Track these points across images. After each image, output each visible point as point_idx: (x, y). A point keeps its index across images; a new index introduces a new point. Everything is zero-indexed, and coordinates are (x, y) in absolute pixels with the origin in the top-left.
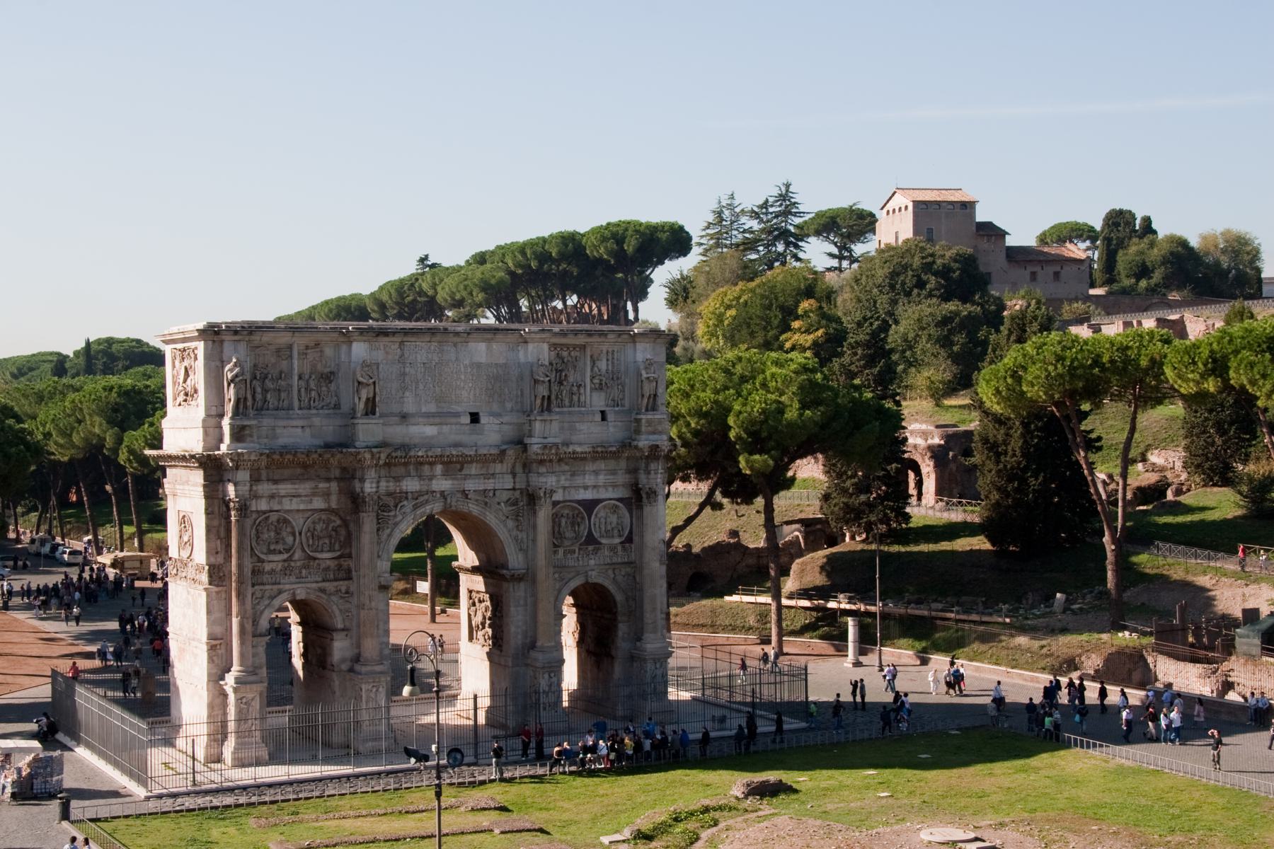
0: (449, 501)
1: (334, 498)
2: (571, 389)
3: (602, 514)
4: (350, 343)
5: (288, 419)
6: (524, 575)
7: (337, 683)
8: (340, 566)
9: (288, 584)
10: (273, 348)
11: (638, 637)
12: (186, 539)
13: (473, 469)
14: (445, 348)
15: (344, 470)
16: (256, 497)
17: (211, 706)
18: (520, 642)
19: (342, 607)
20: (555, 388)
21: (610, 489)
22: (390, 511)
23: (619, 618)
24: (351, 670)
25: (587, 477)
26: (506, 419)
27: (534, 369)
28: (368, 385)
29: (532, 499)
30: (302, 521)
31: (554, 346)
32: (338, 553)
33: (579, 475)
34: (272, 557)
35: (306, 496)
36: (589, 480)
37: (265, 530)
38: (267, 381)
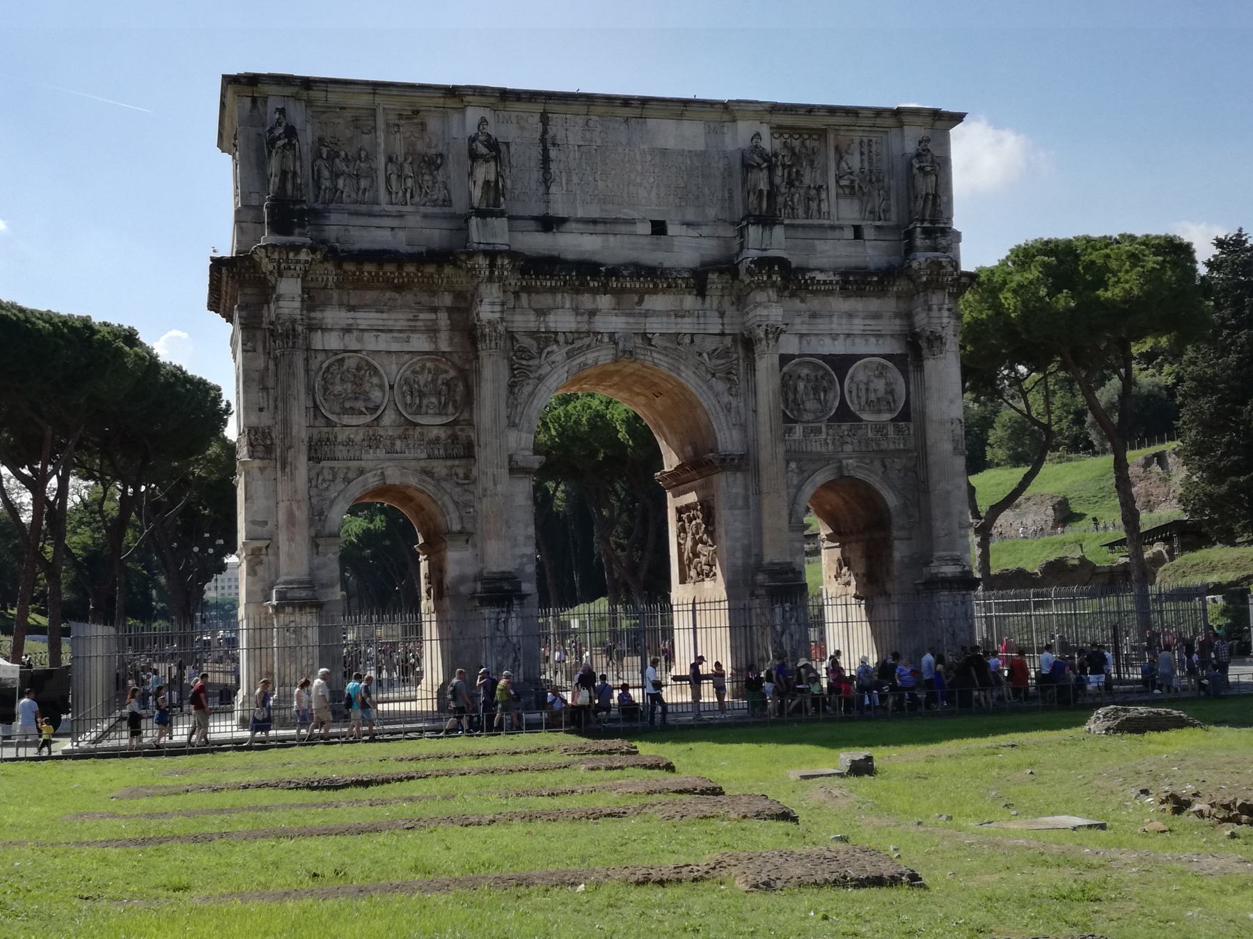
0: (621, 346)
2: (807, 193)
3: (861, 377)
4: (462, 110)
5: (370, 215)
6: (742, 457)
8: (454, 438)
9: (371, 458)
10: (348, 114)
11: (924, 559)
15: (459, 295)
18: (739, 562)
19: (456, 498)
21: (873, 340)
22: (531, 358)
23: (895, 533)
25: (835, 319)
26: (705, 230)
29: (748, 343)
30: (394, 368)
31: (778, 130)
32: (451, 419)
33: (822, 316)
34: (346, 420)
35: (400, 331)
36: (838, 325)
37: (338, 380)
38: (337, 161)
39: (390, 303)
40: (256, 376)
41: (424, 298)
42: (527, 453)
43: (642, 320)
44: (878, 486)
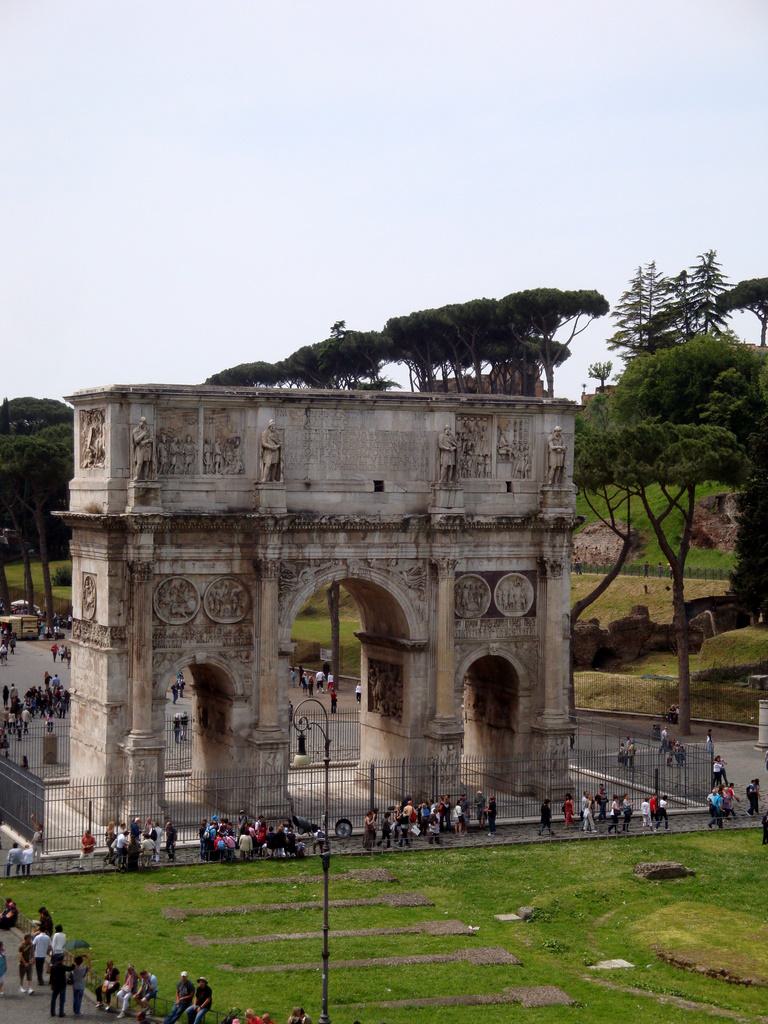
1: (236, 563)
6: (425, 644)
8: (240, 631)
9: (189, 645)
11: (539, 711)
12: (89, 600)
13: (377, 538)
14: (351, 415)
16: (160, 560)
17: (110, 769)
18: (419, 714)
20: (461, 456)
21: (515, 561)
23: (521, 693)
24: (250, 735)
25: (491, 548)
27: (441, 436)
28: (273, 451)
29: (434, 568)
31: (460, 416)
33: (483, 546)
36: (493, 551)
37: (168, 594)
38: (173, 444)
39: (204, 542)
40: (117, 592)
42: (286, 642)
43: (365, 550)
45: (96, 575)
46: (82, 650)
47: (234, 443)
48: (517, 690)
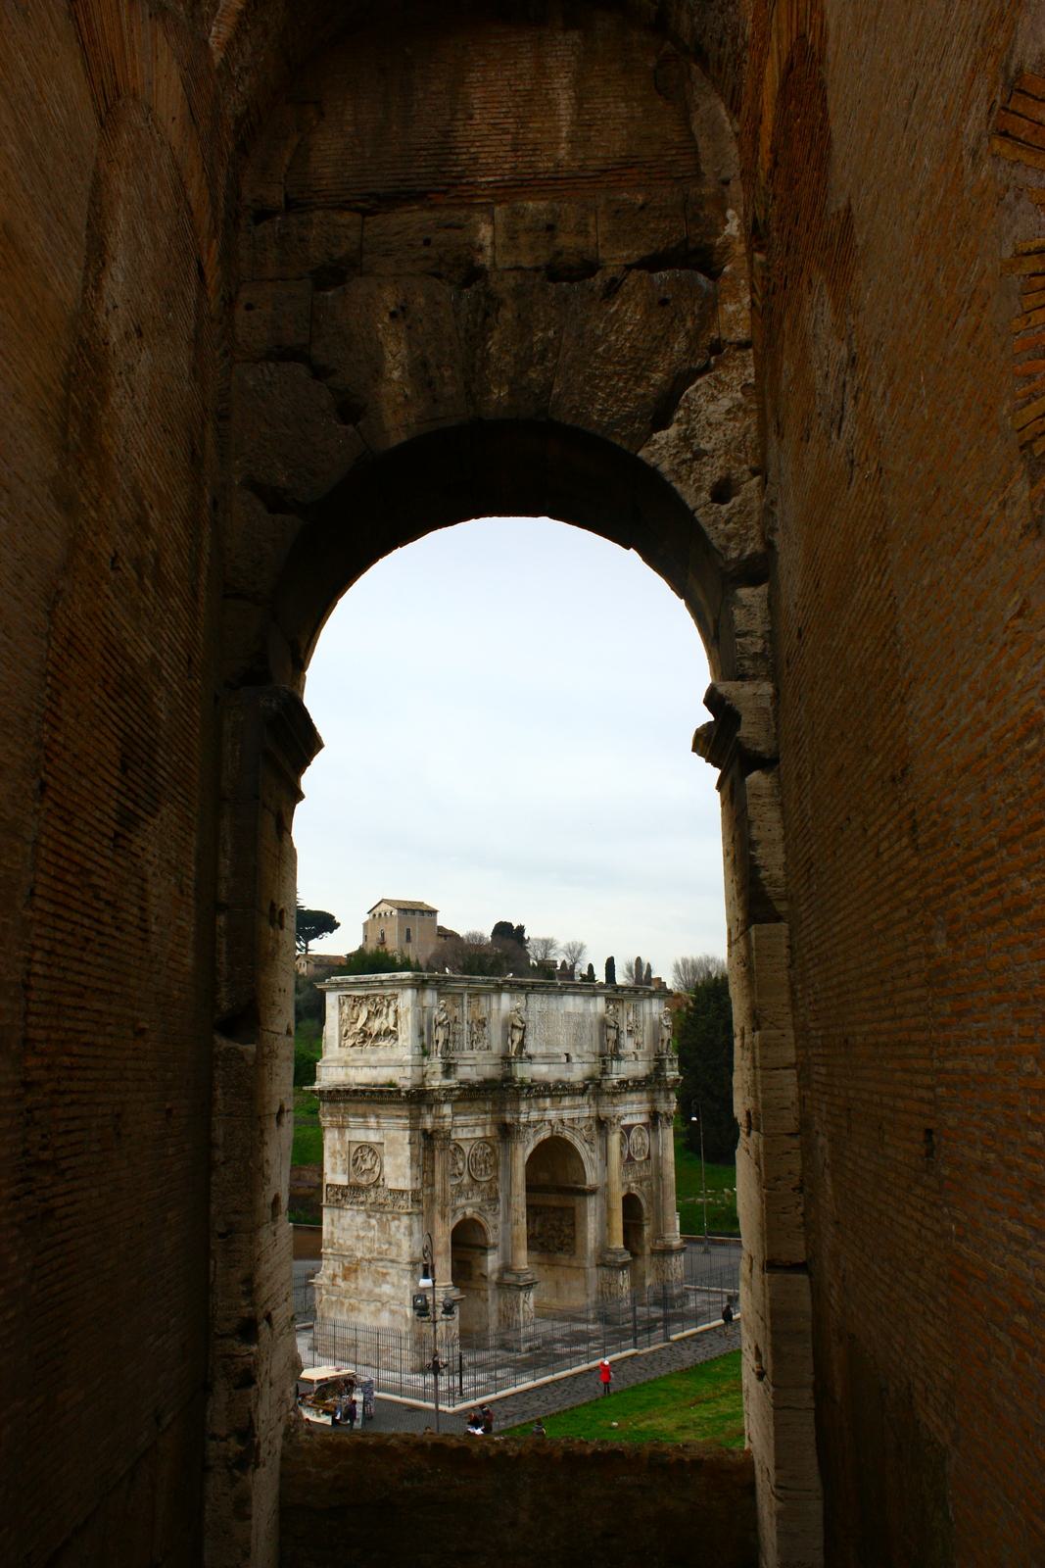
1: (488, 1127)
7: (489, 1292)
8: (491, 1188)
9: (461, 1201)
11: (658, 1234)
13: (567, 1101)
18: (593, 1246)
23: (645, 1222)
24: (501, 1278)
28: (520, 1029)
29: (602, 1125)
36: (629, 1109)
40: (415, 1158)
41: (481, 1105)
44: (639, 1196)
45: (382, 1144)
46: (350, 1213)
47: (482, 1023)
48: (642, 1221)
